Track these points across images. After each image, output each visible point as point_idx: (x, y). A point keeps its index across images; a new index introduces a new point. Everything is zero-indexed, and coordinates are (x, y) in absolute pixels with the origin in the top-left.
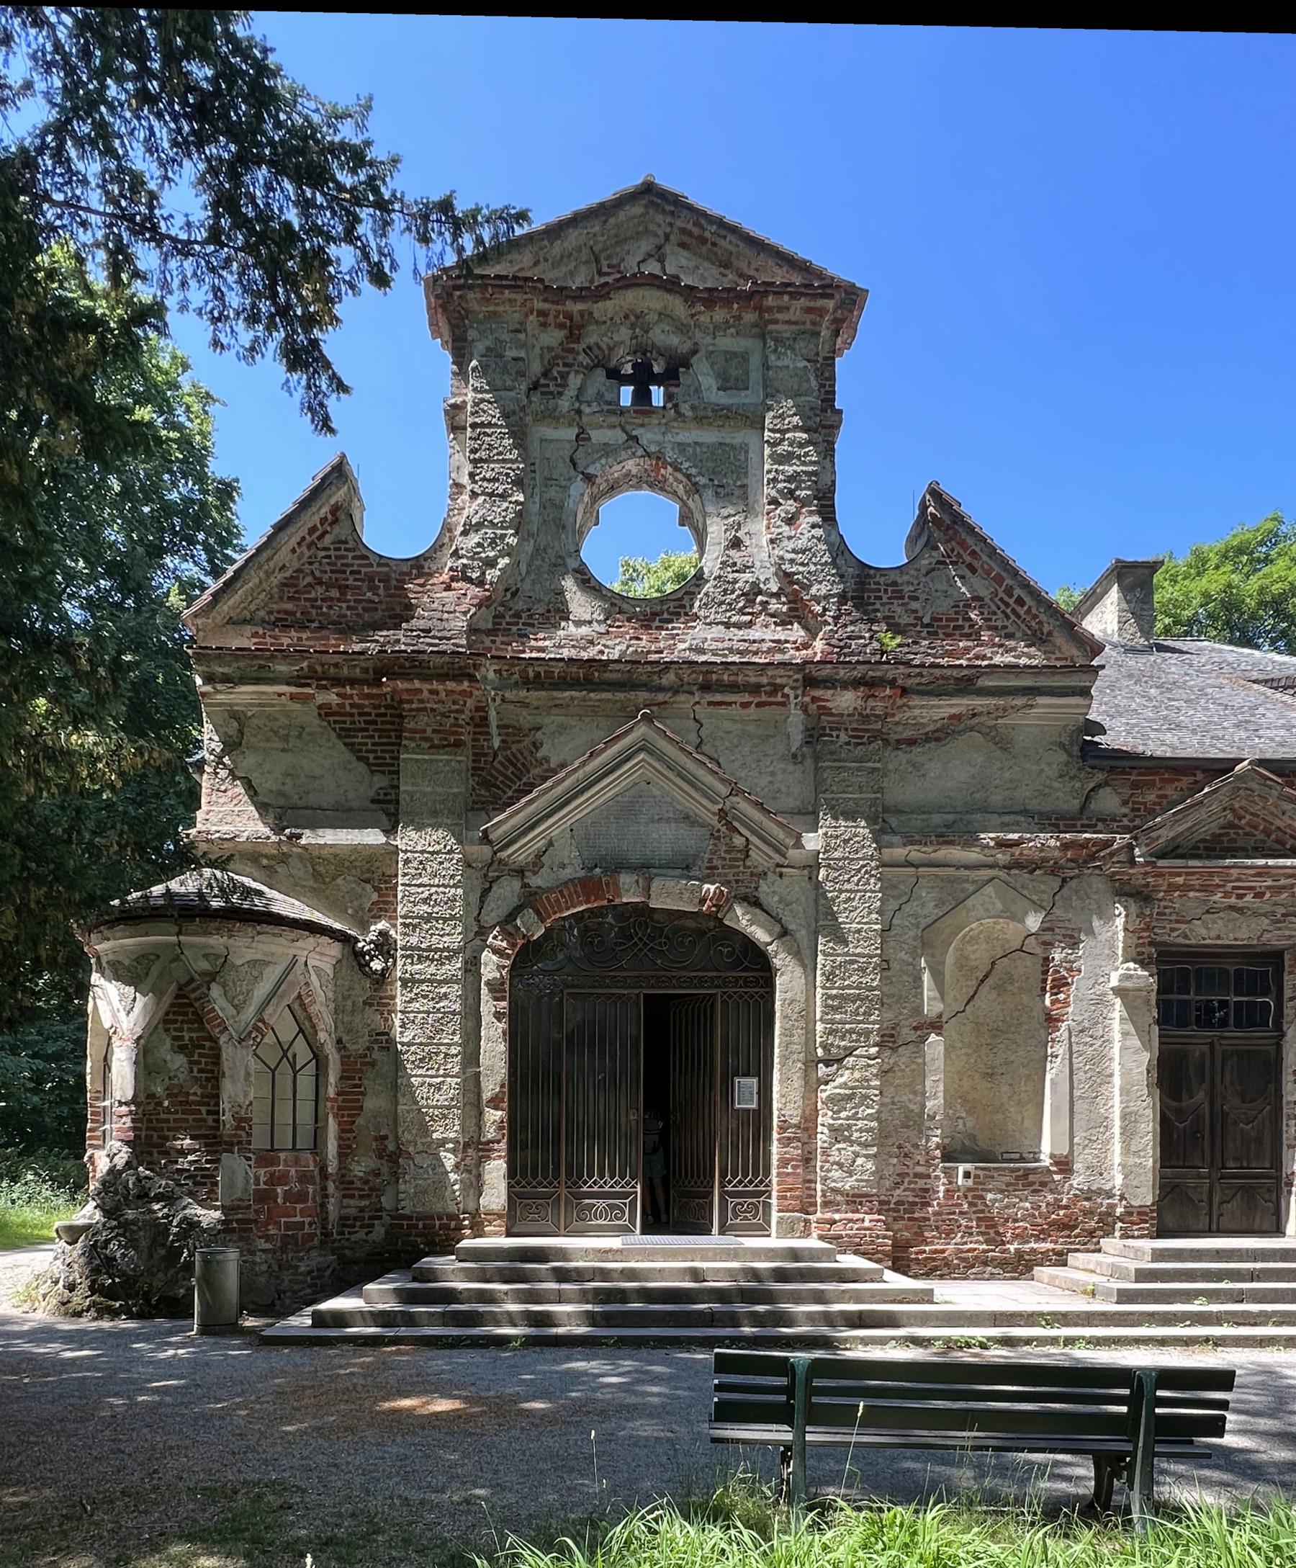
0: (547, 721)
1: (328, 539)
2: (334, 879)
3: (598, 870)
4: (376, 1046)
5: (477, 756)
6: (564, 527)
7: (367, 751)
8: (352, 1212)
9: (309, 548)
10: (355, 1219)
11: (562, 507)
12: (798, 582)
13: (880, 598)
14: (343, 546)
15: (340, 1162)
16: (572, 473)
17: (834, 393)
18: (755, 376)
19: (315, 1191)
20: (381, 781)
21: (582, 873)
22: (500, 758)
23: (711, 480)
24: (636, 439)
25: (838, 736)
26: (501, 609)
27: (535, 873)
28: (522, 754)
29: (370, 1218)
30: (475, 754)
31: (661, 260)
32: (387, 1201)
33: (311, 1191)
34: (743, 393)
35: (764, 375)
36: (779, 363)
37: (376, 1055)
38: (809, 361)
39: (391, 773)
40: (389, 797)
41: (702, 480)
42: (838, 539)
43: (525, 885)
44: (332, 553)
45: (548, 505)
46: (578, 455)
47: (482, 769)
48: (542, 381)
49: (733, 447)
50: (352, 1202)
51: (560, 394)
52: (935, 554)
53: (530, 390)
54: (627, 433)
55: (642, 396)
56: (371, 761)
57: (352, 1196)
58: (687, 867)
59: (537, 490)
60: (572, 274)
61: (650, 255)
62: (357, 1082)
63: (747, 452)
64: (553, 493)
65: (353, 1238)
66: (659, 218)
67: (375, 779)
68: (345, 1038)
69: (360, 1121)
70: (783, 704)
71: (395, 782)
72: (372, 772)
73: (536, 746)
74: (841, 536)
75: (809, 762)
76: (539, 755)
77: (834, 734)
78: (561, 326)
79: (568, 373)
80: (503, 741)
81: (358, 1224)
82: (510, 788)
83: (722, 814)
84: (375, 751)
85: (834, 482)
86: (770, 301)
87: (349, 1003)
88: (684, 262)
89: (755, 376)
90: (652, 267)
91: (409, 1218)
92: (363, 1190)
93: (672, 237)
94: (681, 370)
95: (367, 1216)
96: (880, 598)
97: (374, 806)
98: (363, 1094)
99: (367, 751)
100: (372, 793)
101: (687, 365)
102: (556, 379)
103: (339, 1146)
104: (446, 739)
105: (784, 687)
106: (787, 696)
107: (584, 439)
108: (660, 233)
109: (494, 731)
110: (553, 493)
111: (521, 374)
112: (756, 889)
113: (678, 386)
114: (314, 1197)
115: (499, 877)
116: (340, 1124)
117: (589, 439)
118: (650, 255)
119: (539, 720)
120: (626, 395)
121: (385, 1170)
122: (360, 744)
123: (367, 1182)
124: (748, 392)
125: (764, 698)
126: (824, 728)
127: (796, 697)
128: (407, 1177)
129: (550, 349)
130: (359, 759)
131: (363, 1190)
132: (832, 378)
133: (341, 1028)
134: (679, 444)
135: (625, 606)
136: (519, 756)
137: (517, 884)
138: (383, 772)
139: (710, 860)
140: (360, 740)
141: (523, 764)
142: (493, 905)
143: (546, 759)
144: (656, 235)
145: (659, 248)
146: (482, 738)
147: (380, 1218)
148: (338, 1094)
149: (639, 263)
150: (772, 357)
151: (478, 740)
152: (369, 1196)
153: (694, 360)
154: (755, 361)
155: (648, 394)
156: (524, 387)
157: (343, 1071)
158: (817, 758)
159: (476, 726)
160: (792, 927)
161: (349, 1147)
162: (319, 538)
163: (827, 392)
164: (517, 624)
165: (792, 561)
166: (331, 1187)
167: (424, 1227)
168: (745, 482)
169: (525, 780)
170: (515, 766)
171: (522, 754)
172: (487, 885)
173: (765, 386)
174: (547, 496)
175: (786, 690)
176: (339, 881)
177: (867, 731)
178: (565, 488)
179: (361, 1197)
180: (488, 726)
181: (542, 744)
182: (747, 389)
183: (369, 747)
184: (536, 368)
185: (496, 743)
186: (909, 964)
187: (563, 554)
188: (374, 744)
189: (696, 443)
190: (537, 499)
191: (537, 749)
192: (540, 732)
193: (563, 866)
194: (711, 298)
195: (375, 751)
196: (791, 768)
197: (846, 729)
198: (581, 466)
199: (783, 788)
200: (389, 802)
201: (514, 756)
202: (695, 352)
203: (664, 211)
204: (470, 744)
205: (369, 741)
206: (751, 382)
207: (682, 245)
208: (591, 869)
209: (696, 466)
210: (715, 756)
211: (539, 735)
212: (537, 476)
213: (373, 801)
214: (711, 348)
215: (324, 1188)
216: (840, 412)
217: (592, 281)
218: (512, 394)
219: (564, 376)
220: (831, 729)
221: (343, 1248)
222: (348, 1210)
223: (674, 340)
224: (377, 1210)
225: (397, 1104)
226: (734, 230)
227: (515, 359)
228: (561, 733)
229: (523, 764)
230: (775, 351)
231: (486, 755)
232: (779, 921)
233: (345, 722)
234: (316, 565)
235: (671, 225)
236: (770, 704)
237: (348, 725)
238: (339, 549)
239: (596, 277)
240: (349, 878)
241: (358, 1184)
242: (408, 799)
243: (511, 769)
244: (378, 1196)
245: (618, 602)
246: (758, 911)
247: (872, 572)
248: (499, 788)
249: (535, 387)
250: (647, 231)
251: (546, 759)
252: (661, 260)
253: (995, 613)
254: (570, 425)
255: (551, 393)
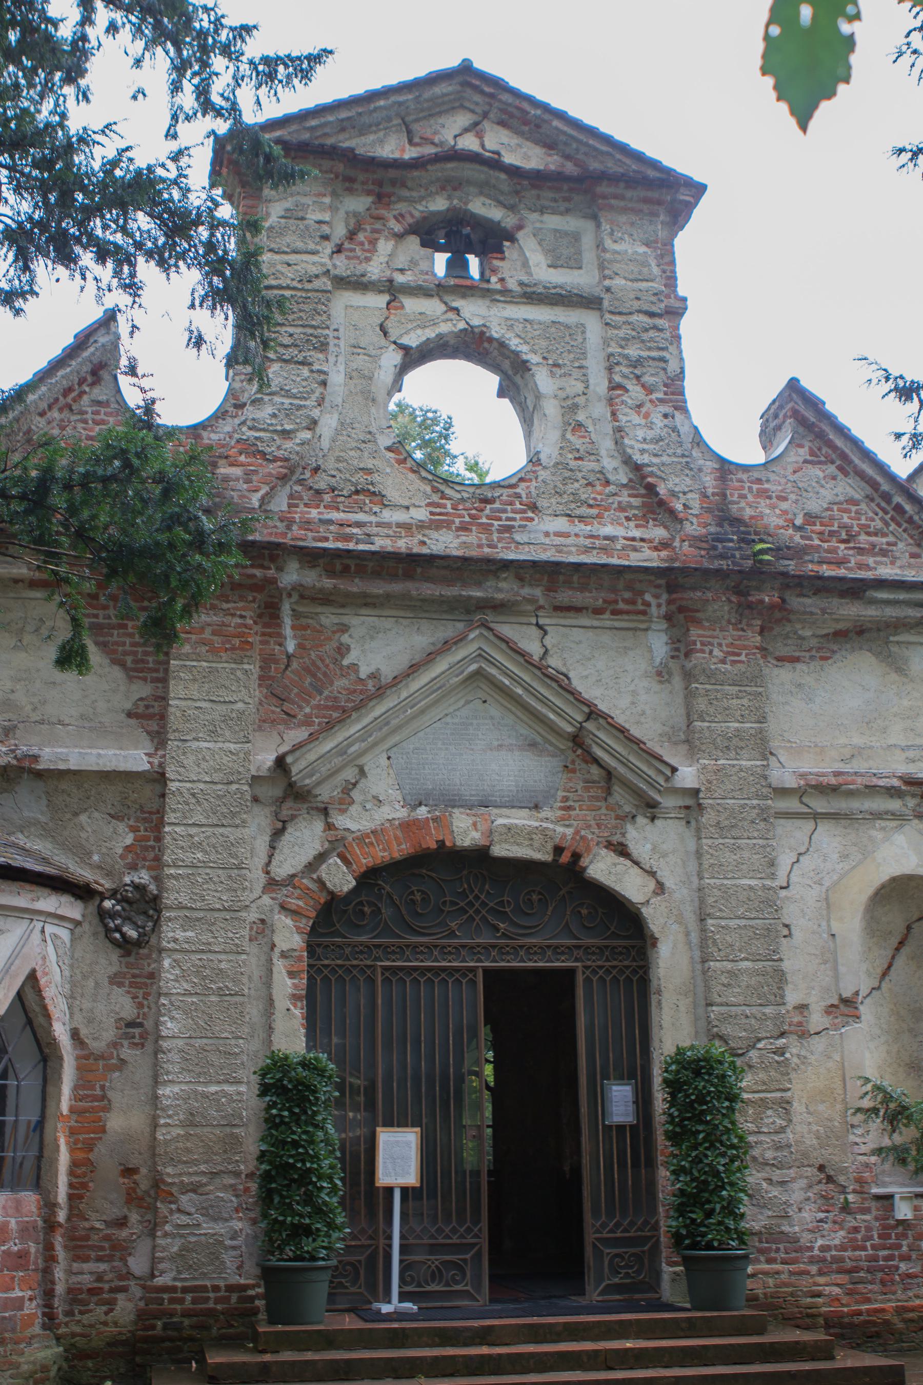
0: (354, 621)
1: (85, 398)
2: (76, 814)
3: (422, 812)
4: (126, 1043)
5: (267, 661)
6: (373, 400)
7: (125, 653)
8: (86, 1280)
9: (61, 410)
10: (91, 1291)
11: (371, 378)
12: (652, 474)
13: (743, 497)
14: (103, 410)
15: (71, 1208)
16: (383, 342)
17: (675, 279)
18: (589, 256)
19: (37, 1251)
20: (143, 690)
21: (402, 813)
22: (295, 665)
23: (545, 358)
24: (457, 310)
25: (711, 652)
26: (298, 488)
27: (343, 811)
28: (323, 661)
29: (112, 1290)
30: (264, 660)
31: (480, 136)
32: (138, 1264)
33: (33, 1250)
34: (576, 272)
35: (598, 257)
36: (617, 247)
37: (126, 1052)
38: (647, 245)
39: (154, 680)
40: (151, 710)
41: (534, 359)
42: (692, 430)
43: (330, 826)
44: (89, 416)
45: (354, 374)
46: (389, 324)
47: (272, 678)
48: (347, 245)
49: (567, 327)
50: (86, 1266)
51: (368, 259)
52: (801, 451)
53: (333, 253)
54: (446, 303)
55: (457, 265)
56: (129, 664)
57: (86, 1259)
58: (536, 807)
59: (341, 359)
60: (381, 142)
61: (466, 130)
62: (98, 1092)
63: (583, 332)
64: (360, 361)
65: (86, 1319)
66: (477, 98)
67: (134, 687)
68: (84, 1032)
69: (101, 1150)
70: (644, 613)
71: (160, 693)
72: (130, 679)
73: (343, 650)
74: (696, 428)
75: (677, 681)
76: (345, 662)
77: (707, 649)
78: (369, 193)
79: (377, 239)
80: (300, 646)
81: (95, 1299)
82: (308, 703)
83: (577, 740)
84: (135, 653)
85: (682, 371)
86: (604, 188)
87: (91, 983)
88: (505, 140)
89: (589, 256)
90: (469, 143)
91: (173, 1289)
92: (102, 1248)
93: (491, 116)
94: (507, 244)
95: (106, 1286)
96: (743, 497)
97: (133, 722)
98: (107, 1109)
99: (125, 653)
100: (128, 706)
101: (512, 239)
102: (362, 244)
103: (71, 1185)
104: (229, 642)
105: (641, 593)
106: (648, 605)
107: (396, 308)
108: (479, 110)
109: (288, 631)
110: (360, 361)
111: (326, 238)
112: (623, 835)
113: (503, 259)
114: (36, 1257)
115: (293, 817)
116: (72, 1151)
117: (403, 307)
118: (466, 130)
119: (345, 620)
120: (441, 261)
121: (134, 1217)
122: (117, 643)
123: (107, 1238)
124: (581, 272)
125: (621, 606)
126: (694, 643)
127: (659, 606)
128: (168, 1228)
129: (355, 214)
130: (114, 662)
131: (102, 1248)
132: (673, 263)
133: (78, 1016)
134: (507, 319)
135: (448, 491)
136: (319, 663)
137: (318, 826)
138: (145, 679)
139: (566, 799)
140: (115, 638)
141: (325, 674)
142: (285, 850)
143: (354, 667)
144: (473, 111)
145: (476, 124)
146: (272, 641)
147: (124, 1289)
148: (72, 1110)
149: (456, 137)
150: (608, 243)
151: (267, 643)
152: (109, 1259)
153: (520, 235)
154: (588, 241)
155: (465, 265)
156: (328, 251)
157: (79, 1079)
158: (688, 676)
159: (266, 625)
160: (669, 883)
161: (84, 1186)
162: (74, 400)
163: (669, 278)
164: (318, 507)
165: (643, 451)
166: (58, 1241)
167: (194, 1301)
168: (584, 363)
169: (326, 693)
170: (314, 676)
171: (323, 661)
172: (279, 825)
173: (602, 267)
174: (354, 365)
175: (648, 597)
176: (83, 818)
177: (745, 647)
178: (375, 358)
179: (99, 1259)
180: (279, 626)
181: (348, 649)
182: (580, 268)
183: (128, 648)
184: (340, 231)
185: (291, 646)
186: (813, 933)
187: (374, 430)
188: (133, 645)
189: (525, 320)
190: (342, 368)
191: (343, 656)
192: (346, 635)
193: (379, 802)
194: (537, 179)
195: (135, 653)
196: (656, 687)
197: (720, 645)
198: (394, 334)
199: (648, 712)
200: (150, 717)
201: (314, 663)
202: (520, 227)
203: (482, 93)
204: (258, 647)
205: (128, 641)
206: (585, 261)
207: (502, 123)
208: (414, 807)
209: (526, 343)
210: (564, 670)
211: (345, 639)
212: (342, 343)
213: (130, 715)
214: (538, 225)
215: (49, 1247)
216: (684, 300)
217: (403, 150)
218: (315, 258)
219: (373, 242)
220: (703, 644)
221: (74, 1335)
222: (80, 1278)
223: (495, 214)
224: (121, 1278)
225: (155, 1126)
226: (561, 115)
227: (320, 222)
228: (372, 638)
229: (325, 674)
230: (612, 234)
231: (276, 662)
232: (652, 874)
233: (96, 616)
234: (69, 430)
235: (490, 105)
236: (628, 612)
237: (101, 620)
238: (97, 413)
239: (407, 146)
240: (96, 814)
241: (95, 1239)
242: (178, 714)
243: (309, 680)
244: (123, 1260)
245: (442, 487)
246: (628, 863)
247: (732, 467)
248: (293, 703)
249: (339, 250)
250: (462, 107)
251: (354, 667)
252: (480, 136)
253: (873, 520)
254: (381, 292)
255: (358, 258)
